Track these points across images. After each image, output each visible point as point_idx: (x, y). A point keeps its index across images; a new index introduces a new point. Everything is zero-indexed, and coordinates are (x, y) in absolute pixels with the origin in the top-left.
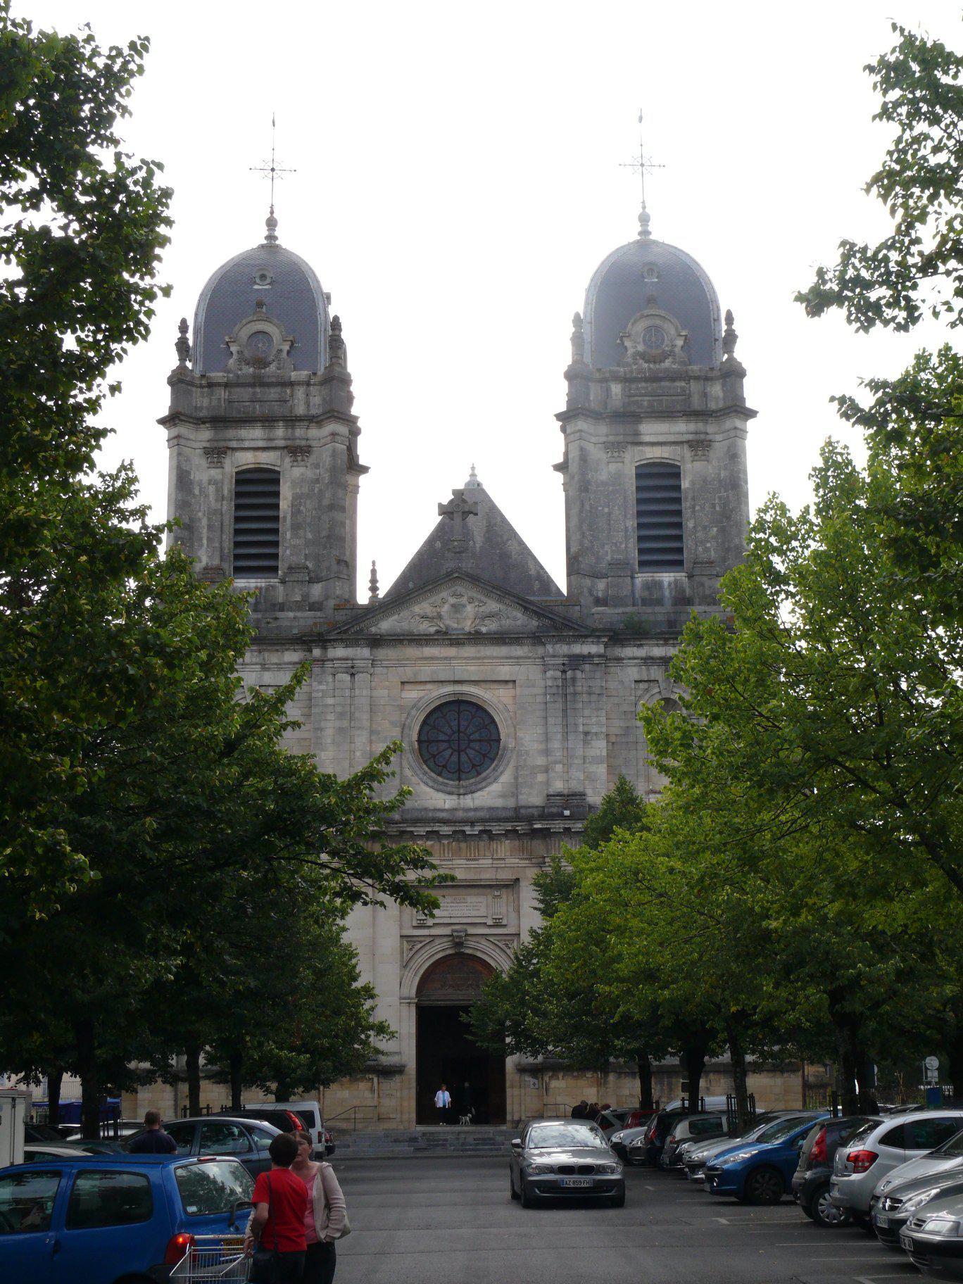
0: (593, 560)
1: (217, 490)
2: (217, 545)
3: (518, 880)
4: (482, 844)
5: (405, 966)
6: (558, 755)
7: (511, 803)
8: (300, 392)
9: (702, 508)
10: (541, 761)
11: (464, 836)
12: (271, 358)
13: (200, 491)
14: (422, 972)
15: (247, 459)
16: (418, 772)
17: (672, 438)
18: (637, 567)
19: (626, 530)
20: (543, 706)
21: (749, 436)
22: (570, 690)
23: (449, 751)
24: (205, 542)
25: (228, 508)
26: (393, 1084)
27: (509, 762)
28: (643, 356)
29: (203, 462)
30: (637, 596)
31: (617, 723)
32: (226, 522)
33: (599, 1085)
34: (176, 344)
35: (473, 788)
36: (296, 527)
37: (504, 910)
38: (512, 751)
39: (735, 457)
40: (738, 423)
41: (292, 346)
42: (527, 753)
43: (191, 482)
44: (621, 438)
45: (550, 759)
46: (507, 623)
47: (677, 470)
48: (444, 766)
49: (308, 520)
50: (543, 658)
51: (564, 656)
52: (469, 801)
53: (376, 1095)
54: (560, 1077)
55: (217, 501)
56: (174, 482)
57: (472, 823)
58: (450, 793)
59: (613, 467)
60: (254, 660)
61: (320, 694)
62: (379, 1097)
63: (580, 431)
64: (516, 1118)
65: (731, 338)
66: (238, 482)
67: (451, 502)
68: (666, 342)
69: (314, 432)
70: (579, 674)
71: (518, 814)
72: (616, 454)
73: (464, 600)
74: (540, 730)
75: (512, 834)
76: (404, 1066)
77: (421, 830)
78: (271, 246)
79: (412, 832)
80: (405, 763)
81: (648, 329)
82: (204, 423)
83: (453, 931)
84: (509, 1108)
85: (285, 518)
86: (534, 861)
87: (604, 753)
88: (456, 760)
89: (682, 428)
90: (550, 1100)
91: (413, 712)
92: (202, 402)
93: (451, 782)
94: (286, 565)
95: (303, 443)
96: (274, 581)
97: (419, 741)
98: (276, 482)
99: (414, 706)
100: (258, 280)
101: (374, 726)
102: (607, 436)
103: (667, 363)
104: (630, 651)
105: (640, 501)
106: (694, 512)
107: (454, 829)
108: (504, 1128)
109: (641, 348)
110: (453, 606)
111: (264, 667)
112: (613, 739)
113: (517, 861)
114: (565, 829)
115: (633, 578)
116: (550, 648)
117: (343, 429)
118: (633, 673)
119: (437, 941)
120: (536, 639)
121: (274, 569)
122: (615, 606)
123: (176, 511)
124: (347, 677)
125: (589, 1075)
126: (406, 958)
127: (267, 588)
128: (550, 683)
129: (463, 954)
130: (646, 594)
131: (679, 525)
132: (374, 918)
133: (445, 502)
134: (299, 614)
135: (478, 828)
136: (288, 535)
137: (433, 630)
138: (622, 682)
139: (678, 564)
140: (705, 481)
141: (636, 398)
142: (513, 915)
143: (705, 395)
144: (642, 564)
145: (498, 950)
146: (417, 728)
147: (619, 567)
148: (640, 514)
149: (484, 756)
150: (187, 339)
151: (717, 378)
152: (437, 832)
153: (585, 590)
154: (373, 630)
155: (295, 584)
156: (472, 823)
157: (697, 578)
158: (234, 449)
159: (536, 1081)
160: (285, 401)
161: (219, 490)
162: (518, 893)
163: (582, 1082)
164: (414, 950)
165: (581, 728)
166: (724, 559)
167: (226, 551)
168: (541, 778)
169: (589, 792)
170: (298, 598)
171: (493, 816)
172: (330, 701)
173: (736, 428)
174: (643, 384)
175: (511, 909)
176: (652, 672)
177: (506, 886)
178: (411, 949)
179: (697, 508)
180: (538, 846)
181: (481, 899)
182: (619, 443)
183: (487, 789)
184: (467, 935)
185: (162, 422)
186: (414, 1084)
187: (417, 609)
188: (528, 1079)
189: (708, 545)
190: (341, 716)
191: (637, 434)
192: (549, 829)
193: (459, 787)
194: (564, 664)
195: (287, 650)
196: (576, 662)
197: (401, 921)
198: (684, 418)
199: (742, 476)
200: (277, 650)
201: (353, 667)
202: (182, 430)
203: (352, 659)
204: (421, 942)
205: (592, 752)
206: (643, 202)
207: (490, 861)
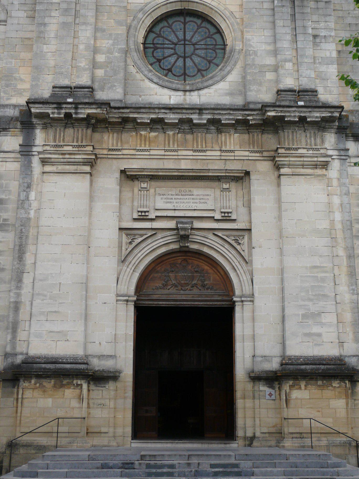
3: (247, 173)
4: (209, 136)
6: (289, 54)
7: (239, 101)
10: (270, 61)
16: (143, 69)
20: (270, 12)
27: (236, 63)
35: (200, 85)
37: (233, 203)
42: (255, 53)
45: (279, 57)
48: (170, 70)
53: (85, 404)
54: (303, 387)
62: (89, 407)
64: (249, 434)
74: (268, 33)
76: (120, 372)
79: (135, 119)
80: (129, 61)
84: (240, 422)
86: (265, 154)
88: (187, 33)
90: (291, 413)
91: (140, 15)
97: (144, 44)
99: (141, 10)
101: (100, 25)
107: (180, 116)
108: (234, 445)
113: (247, 153)
114: (300, 117)
119: (160, 235)
125: (336, 384)
126: (124, 253)
132: (91, 208)
135: (206, 117)
142: (243, 211)
145: (227, 246)
149: (210, 62)
159: (273, 392)
163: (328, 393)
164: (134, 244)
165: (310, 31)
169: (320, 90)
175: (240, 204)
178: (130, 243)
181: (208, 192)
183: (214, 87)
184: (192, 229)
186: (130, 393)
188: (263, 388)
192: (284, 117)
197: (120, 212)
204: (141, 235)
207: (218, 153)
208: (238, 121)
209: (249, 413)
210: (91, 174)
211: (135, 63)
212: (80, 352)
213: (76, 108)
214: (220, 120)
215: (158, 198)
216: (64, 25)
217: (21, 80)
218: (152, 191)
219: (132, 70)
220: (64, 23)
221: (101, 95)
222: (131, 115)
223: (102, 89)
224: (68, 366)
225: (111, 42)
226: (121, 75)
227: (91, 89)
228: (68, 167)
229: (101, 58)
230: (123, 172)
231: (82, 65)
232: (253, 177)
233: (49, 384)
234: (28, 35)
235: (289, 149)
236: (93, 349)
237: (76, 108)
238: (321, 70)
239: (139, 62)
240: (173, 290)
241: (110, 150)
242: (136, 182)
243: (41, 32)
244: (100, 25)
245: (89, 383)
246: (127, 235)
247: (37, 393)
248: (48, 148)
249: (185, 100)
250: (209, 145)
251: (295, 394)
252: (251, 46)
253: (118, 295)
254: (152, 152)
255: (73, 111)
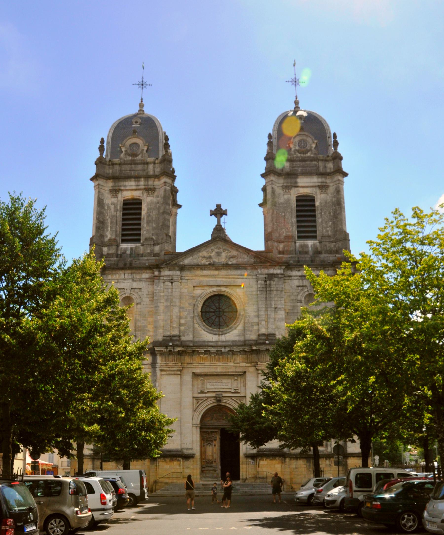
0: (278, 235)
1: (115, 207)
2: (114, 229)
4: (229, 356)
5: (194, 411)
6: (263, 317)
7: (242, 339)
8: (151, 166)
9: (325, 213)
10: (256, 320)
11: (222, 353)
12: (139, 153)
13: (108, 207)
14: (202, 413)
15: (128, 195)
17: (311, 184)
18: (297, 238)
19: (292, 223)
20: (256, 296)
21: (345, 184)
22: (268, 289)
23: (215, 317)
24: (109, 229)
25: (119, 215)
26: (189, 463)
27: (241, 321)
28: (298, 151)
29: (109, 196)
30: (297, 250)
31: (289, 304)
32: (118, 220)
33: (282, 463)
34: (99, 148)
35: (225, 332)
36: (148, 222)
37: (239, 385)
38: (242, 316)
39: (339, 192)
40: (340, 178)
41: (148, 148)
42: (249, 316)
43: (104, 204)
44: (289, 184)
45: (259, 319)
46: (240, 260)
47: (313, 198)
48: (213, 323)
49: (154, 219)
50: (256, 275)
51: (266, 274)
52: (223, 338)
53: (182, 467)
54: (265, 460)
55: (114, 211)
56: (96, 203)
57: (225, 347)
58: (215, 334)
59: (286, 196)
60: (129, 277)
61: (158, 291)
63: (272, 180)
64: (245, 478)
65: (336, 144)
66: (124, 204)
67: (216, 210)
68: (308, 146)
69: (157, 182)
70: (272, 282)
71: (245, 343)
72: (287, 191)
73: (222, 250)
74: (255, 307)
75: (243, 352)
76: (194, 455)
77: (202, 350)
78: (141, 111)
79: (198, 351)
80: (195, 322)
81: (300, 141)
82: (109, 179)
83: (216, 395)
84: (241, 473)
85: (144, 218)
86: (253, 364)
87: (284, 316)
89: (315, 180)
90: (260, 470)
91: (199, 299)
92: (109, 171)
93: (215, 330)
94: (144, 238)
95: (152, 187)
96: (139, 245)
97: (202, 312)
98: (140, 204)
99: (199, 296)
100: (134, 123)
102: (283, 183)
103: (309, 154)
104: (294, 273)
105: (298, 211)
106: (321, 215)
107: (216, 349)
108: (238, 482)
109: (297, 148)
110: (217, 253)
111: (134, 280)
112: (287, 311)
113: (245, 364)
115: (295, 243)
116: (259, 271)
117: (169, 181)
118: (296, 282)
119: (209, 400)
120: (254, 266)
121: (139, 240)
122: (288, 254)
123: (97, 215)
124: (169, 284)
125: (277, 459)
127: (136, 248)
128: (259, 286)
129: (220, 405)
130: (301, 250)
131: (315, 221)
132: (181, 389)
133: (213, 209)
134: (149, 258)
136: (145, 225)
137: (207, 263)
138: (291, 286)
139: (315, 237)
140: (326, 202)
141: (295, 168)
142: (243, 388)
143: (325, 167)
144: (299, 237)
146: (200, 306)
147: (289, 238)
148: (298, 216)
150: (104, 146)
151: (330, 160)
152: (209, 351)
153: (275, 248)
154: (181, 263)
155: (148, 246)
156: (225, 347)
157: (323, 243)
158: (122, 190)
159: (254, 462)
160: (145, 170)
161: (116, 207)
162: (246, 378)
163: (274, 462)
164: (199, 403)
165: (273, 306)
166: (335, 235)
167: (118, 232)
168: (256, 327)
169: (277, 333)
170: (149, 251)
171: (234, 344)
172: (162, 294)
173: (339, 180)
174: (299, 163)
175: (242, 385)
176: (304, 282)
177: (240, 375)
178: (197, 403)
179: (323, 213)
180: (254, 357)
181: (229, 381)
182: (288, 186)
184: (222, 397)
185: (92, 179)
187: (200, 254)
188: (250, 460)
189: (328, 229)
190: (167, 300)
191: (296, 183)
192: (259, 349)
193: (219, 332)
194: (265, 278)
195: (144, 273)
196: (271, 277)
198: (317, 176)
199: (342, 200)
200: (139, 273)
201: (172, 279)
202: (101, 181)
203: (172, 276)
204: (202, 400)
205: (278, 316)
206: (296, 96)
207: (233, 364)
208: (241, 350)
209: (245, 470)
210: (180, 375)
211: (197, 322)
212: (179, 447)
213: (174, 348)
214: (233, 350)
215: (208, 384)
216: (166, 307)
217: (149, 331)
218: (206, 381)
219: (196, 325)
220: (166, 306)
221: (183, 339)
222: (196, 349)
223: (184, 336)
224: (175, 453)
225: (187, 313)
226: (191, 329)
227: (179, 336)
228: (171, 372)
229: (183, 321)
230: (193, 373)
231: (175, 325)
232: (247, 374)
233: (168, 460)
234: (151, 310)
235: (262, 362)
236: (184, 446)
237: (174, 348)
238: (278, 324)
239: (199, 322)
240: (215, 421)
241: (188, 364)
242: (199, 377)
243: (157, 310)
244: (182, 305)
245: (183, 459)
246: (196, 400)
247: (164, 463)
248: (163, 364)
249: (219, 339)
250: (229, 360)
251: (262, 463)
252: (247, 313)
253: (193, 425)
254: (206, 364)
255: (172, 349)
